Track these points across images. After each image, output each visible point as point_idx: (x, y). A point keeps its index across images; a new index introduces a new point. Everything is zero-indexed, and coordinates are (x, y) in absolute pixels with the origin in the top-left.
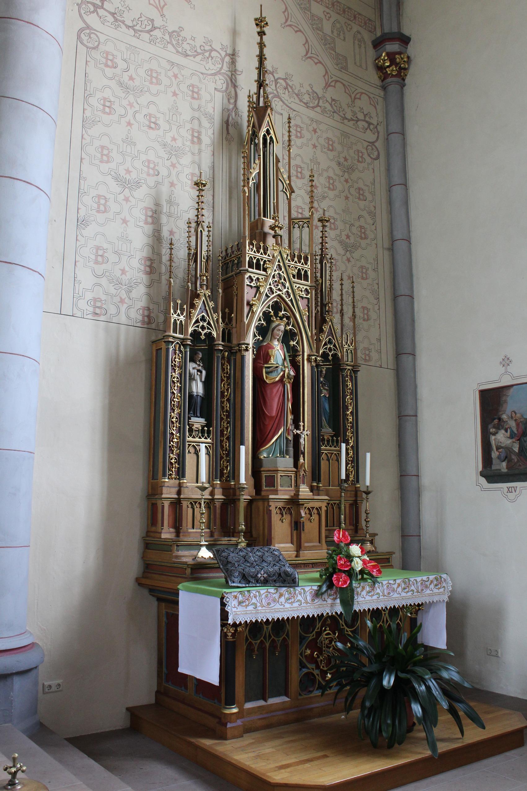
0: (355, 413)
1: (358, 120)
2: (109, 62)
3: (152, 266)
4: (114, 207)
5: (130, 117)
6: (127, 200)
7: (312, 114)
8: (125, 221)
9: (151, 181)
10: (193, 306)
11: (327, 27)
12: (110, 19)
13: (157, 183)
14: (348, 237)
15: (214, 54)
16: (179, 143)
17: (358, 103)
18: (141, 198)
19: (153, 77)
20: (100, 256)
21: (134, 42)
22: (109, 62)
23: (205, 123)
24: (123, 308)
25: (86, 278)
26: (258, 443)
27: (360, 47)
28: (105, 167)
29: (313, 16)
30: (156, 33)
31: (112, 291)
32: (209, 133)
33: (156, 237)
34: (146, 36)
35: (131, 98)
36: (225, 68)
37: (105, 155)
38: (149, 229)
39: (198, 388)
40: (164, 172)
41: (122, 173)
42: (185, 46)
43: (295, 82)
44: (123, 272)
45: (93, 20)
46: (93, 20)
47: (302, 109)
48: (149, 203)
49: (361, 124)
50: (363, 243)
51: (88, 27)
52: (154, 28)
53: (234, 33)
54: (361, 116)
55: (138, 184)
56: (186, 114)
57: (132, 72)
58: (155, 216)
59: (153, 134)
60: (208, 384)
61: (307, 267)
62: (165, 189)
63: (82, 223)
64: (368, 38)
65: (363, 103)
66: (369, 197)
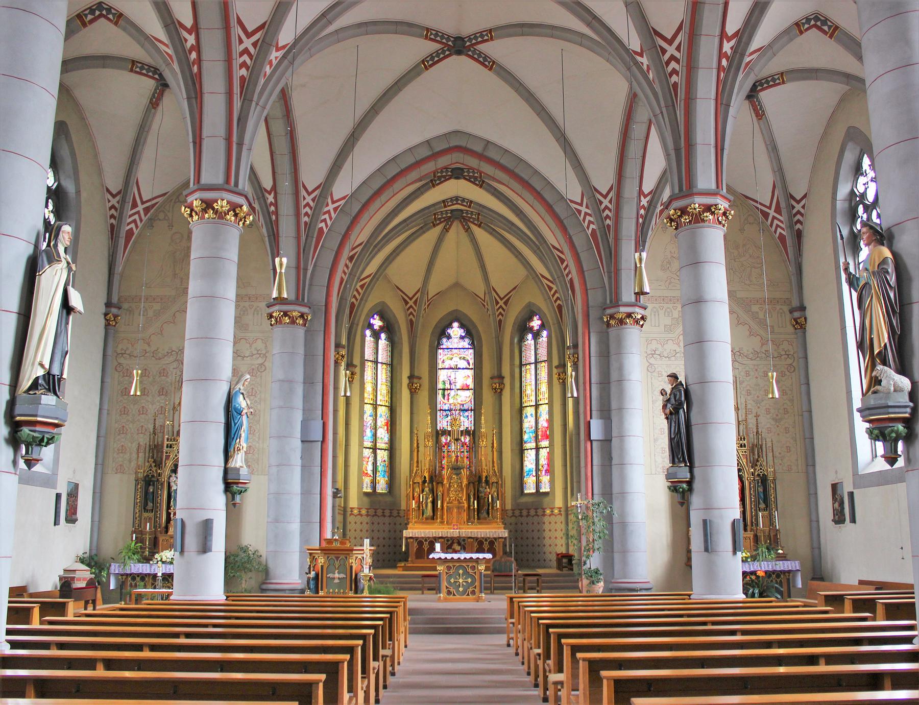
0: (776, 498)
7: (755, 362)
17: (782, 347)
21: (669, 362)
34: (673, 358)
43: (745, 351)
45: (652, 361)
47: (749, 362)
50: (786, 416)
54: (783, 353)
61: (745, 442)
63: (655, 440)
64: (786, 309)
65: (785, 346)
66: (789, 392)
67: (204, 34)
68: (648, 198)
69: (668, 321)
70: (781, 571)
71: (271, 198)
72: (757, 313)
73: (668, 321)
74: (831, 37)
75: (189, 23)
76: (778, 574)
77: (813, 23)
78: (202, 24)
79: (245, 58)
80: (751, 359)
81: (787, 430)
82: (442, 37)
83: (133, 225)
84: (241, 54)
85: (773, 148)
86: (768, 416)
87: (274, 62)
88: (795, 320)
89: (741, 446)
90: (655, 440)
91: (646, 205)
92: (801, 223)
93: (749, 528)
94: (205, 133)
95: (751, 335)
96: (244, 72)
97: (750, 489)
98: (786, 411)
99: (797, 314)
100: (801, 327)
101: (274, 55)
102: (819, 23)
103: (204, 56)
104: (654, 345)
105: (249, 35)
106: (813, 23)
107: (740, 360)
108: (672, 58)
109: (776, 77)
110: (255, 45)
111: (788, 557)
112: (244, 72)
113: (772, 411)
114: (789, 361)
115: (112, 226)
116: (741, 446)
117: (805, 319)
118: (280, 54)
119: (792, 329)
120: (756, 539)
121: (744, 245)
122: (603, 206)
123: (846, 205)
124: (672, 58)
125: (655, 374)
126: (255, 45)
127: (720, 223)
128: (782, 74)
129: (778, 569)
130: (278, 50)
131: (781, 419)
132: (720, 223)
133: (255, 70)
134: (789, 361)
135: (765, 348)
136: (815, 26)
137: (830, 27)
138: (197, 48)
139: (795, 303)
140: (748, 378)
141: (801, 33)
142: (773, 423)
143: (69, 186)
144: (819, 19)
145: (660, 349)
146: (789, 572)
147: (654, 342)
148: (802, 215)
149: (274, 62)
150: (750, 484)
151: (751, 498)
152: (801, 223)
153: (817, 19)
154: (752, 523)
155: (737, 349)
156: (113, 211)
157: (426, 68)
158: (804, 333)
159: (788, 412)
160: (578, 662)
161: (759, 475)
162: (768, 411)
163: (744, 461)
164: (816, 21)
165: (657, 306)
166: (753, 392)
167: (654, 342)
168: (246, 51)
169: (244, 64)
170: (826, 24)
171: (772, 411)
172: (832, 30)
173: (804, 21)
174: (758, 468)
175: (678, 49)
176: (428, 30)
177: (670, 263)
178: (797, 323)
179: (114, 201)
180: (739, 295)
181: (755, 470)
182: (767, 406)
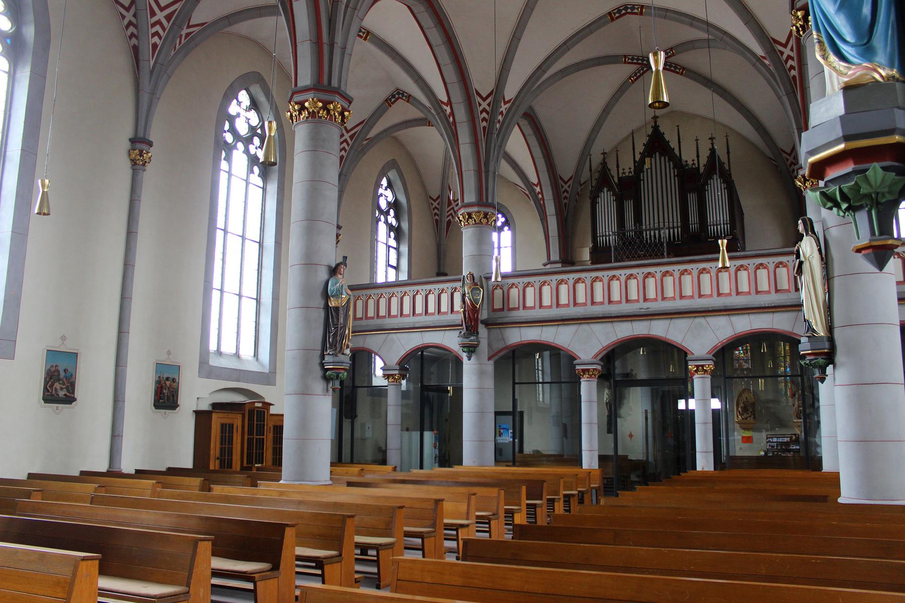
67: (454, 106)
71: (538, 189)
75: (445, 99)
78: (453, 100)
79: (484, 115)
82: (638, 59)
83: (450, 217)
84: (481, 112)
87: (504, 112)
94: (463, 169)
96: (484, 124)
101: (504, 108)
103: (457, 120)
105: (484, 99)
108: (789, 57)
110: (489, 105)
112: (484, 124)
115: (437, 220)
118: (508, 105)
122: (789, 162)
124: (789, 57)
126: (489, 105)
130: (505, 103)
133: (491, 121)
138: (452, 113)
143: (403, 199)
149: (504, 112)
156: (436, 211)
157: (633, 82)
168: (484, 110)
169: (484, 119)
175: (792, 50)
176: (625, 57)
179: (435, 204)
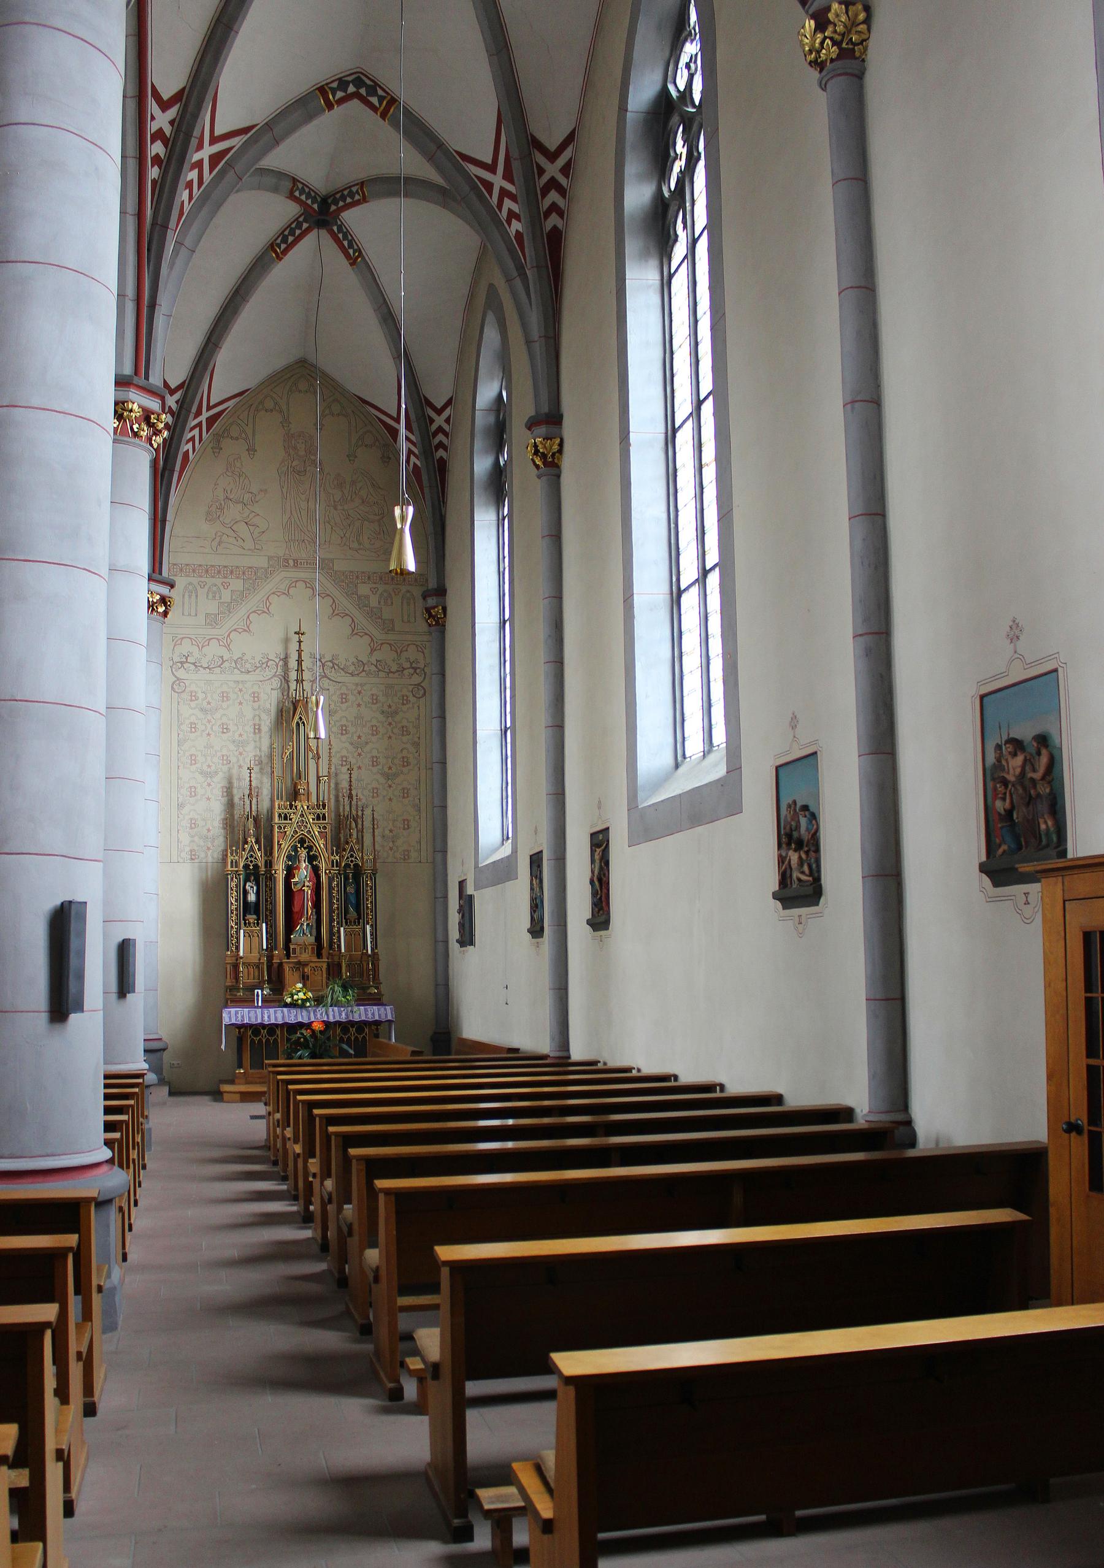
0: (375, 903)
1: (404, 669)
2: (193, 697)
3: (229, 824)
4: (200, 791)
5: (209, 730)
6: (209, 785)
7: (356, 679)
8: (208, 799)
9: (225, 768)
10: (244, 850)
11: (374, 601)
12: (193, 667)
13: (230, 769)
14: (390, 768)
15: (270, 663)
16: (245, 737)
18: (218, 784)
19: (224, 697)
20: (193, 824)
21: (212, 677)
22: (193, 697)
23: (264, 716)
24: (209, 853)
25: (185, 838)
26: (290, 927)
27: (408, 604)
28: (193, 768)
29: (359, 597)
30: (226, 664)
31: (202, 843)
32: (267, 721)
33: (230, 805)
34: (218, 670)
35: (209, 717)
36: (279, 670)
37: (193, 759)
38: (224, 800)
39: (252, 898)
40: (234, 760)
41: (205, 768)
42: (248, 666)
44: (209, 830)
45: (181, 674)
46: (181, 674)
47: (348, 679)
48: (224, 783)
49: (406, 672)
50: (405, 770)
51: (178, 679)
52: (223, 662)
53: (287, 641)
55: (216, 773)
56: (249, 713)
57: (209, 698)
58: (229, 791)
59: (225, 736)
60: (258, 894)
62: (235, 771)
63: (180, 806)
64: (417, 592)
65: (412, 653)
68: (178, 396)
69: (212, 607)
70: (365, 1023)
72: (367, 597)
73: (212, 607)
74: (383, 116)
76: (361, 1025)
77: (351, 89)
80: (352, 675)
81: (405, 793)
85: (388, 318)
86: (375, 770)
88: (428, 610)
89: (318, 818)
90: (180, 806)
91: (174, 407)
92: (445, 449)
93: (324, 952)
95: (354, 633)
97: (330, 888)
98: (406, 762)
99: (431, 602)
100: (437, 623)
102: (363, 91)
104: (186, 647)
106: (351, 89)
107: (332, 674)
109: (354, 189)
111: (384, 999)
113: (382, 760)
114: (416, 679)
116: (318, 818)
117: (444, 609)
119: (425, 625)
120: (334, 971)
121: (353, 483)
123: (492, 419)
125: (185, 696)
127: (136, 435)
128: (362, 184)
129: (357, 1018)
131: (396, 775)
132: (136, 435)
134: (416, 679)
135: (377, 655)
136: (357, 95)
137: (381, 99)
139: (432, 584)
140: (344, 706)
141: (330, 106)
142: (382, 780)
144: (364, 84)
145: (196, 653)
146: (377, 1023)
147: (186, 642)
148: (446, 434)
150: (331, 880)
151: (331, 904)
152: (445, 449)
153: (358, 82)
154: (331, 946)
155: (328, 657)
158: (443, 633)
159: (408, 764)
160: (351, 1161)
161: (347, 866)
162: (375, 762)
163: (322, 842)
164: (358, 87)
165: (195, 580)
166: (351, 729)
167: (186, 642)
170: (375, 94)
171: (382, 760)
172: (387, 106)
173: (335, 85)
174: (346, 854)
177: (221, 508)
178: (430, 615)
180: (340, 566)
181: (341, 857)
182: (375, 753)
